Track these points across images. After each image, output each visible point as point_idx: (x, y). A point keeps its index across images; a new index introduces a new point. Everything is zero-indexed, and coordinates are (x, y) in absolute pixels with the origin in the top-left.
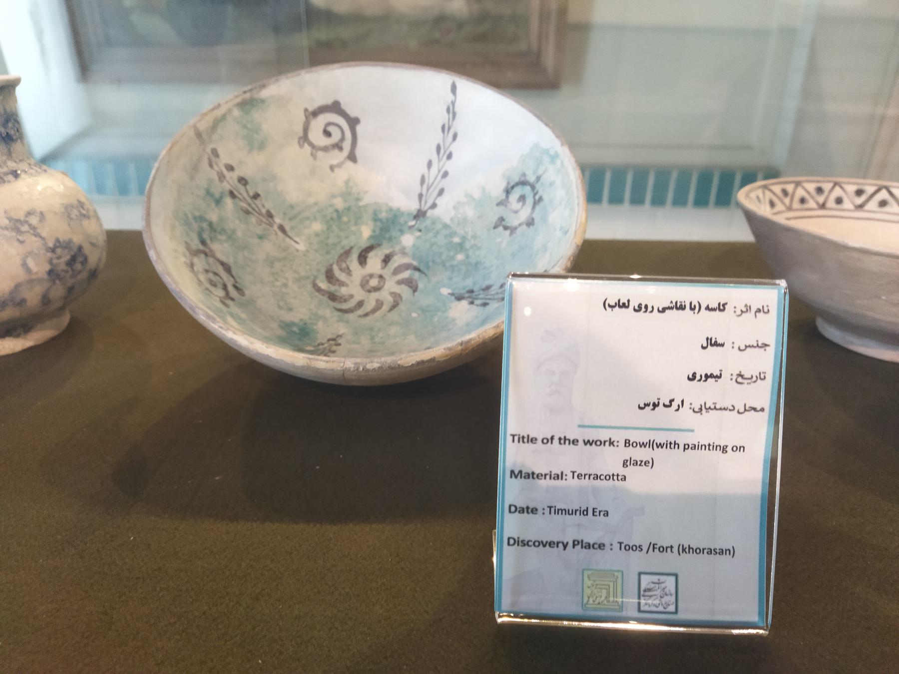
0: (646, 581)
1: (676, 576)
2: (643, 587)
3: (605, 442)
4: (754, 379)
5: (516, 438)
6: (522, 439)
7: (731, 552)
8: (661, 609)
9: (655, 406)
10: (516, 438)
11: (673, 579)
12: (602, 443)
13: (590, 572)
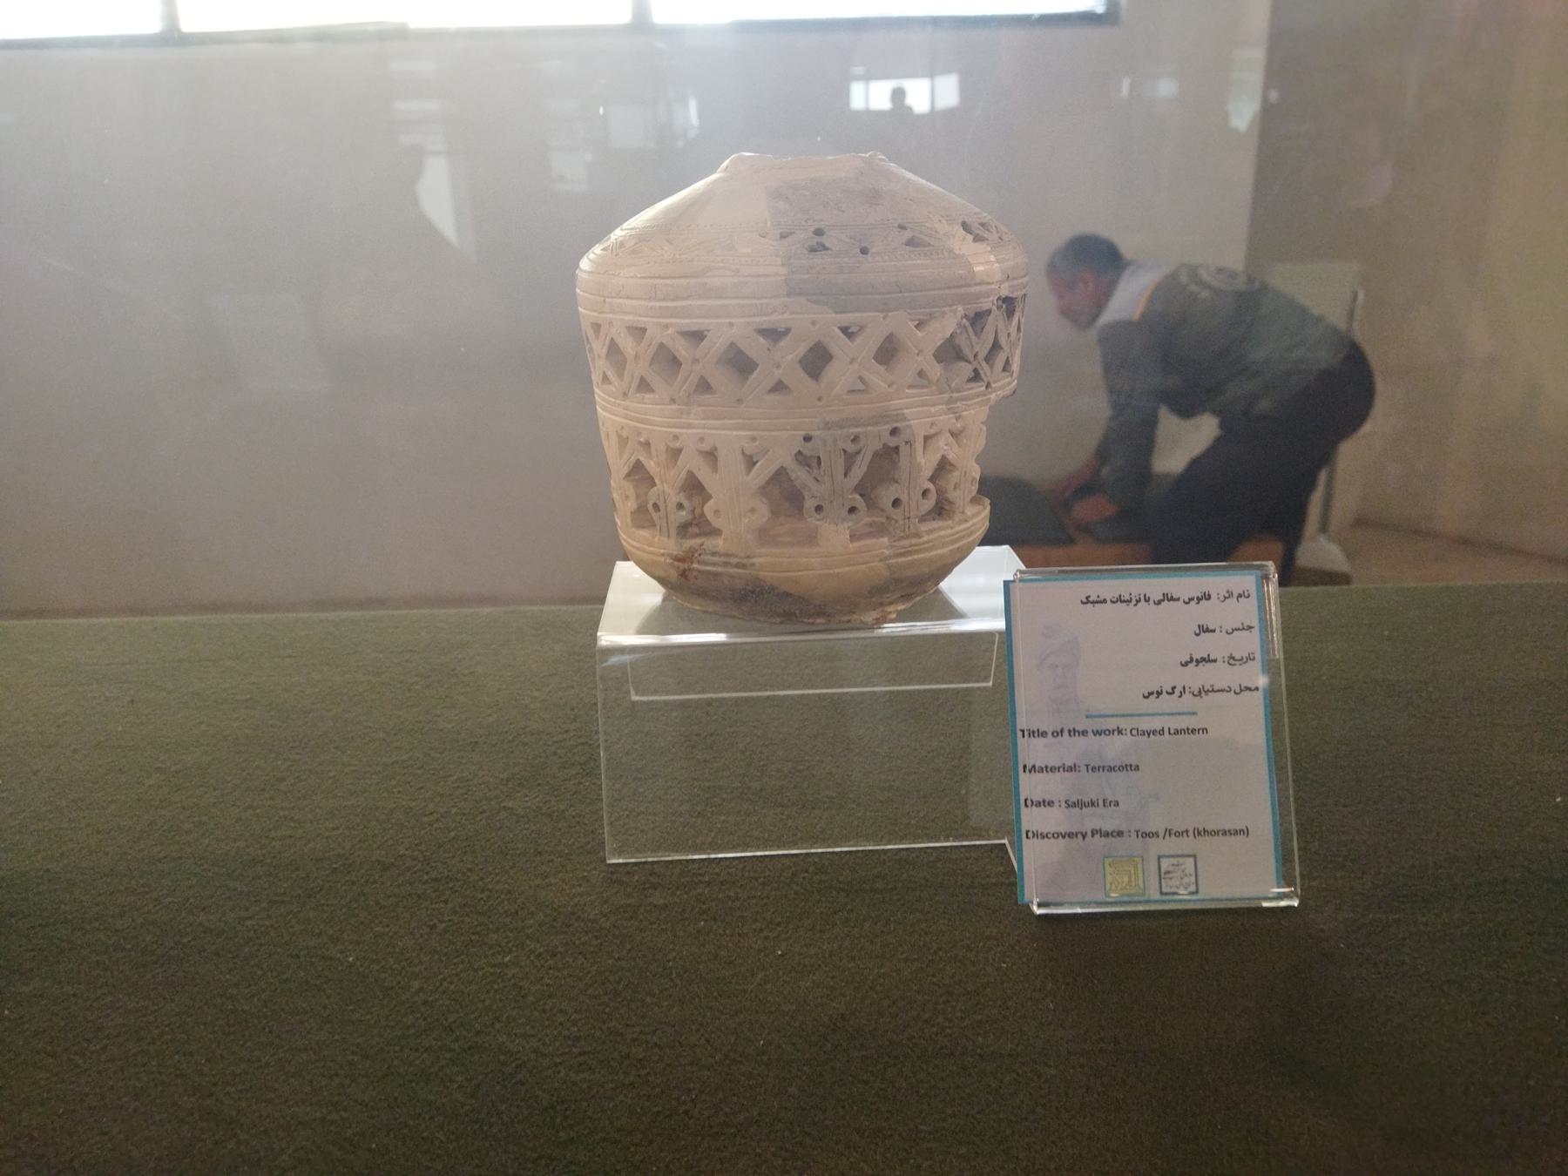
0: (1165, 864)
1: (1195, 857)
6: (1032, 734)
7: (1245, 832)
9: (1159, 694)
11: (1191, 860)
12: (1111, 732)
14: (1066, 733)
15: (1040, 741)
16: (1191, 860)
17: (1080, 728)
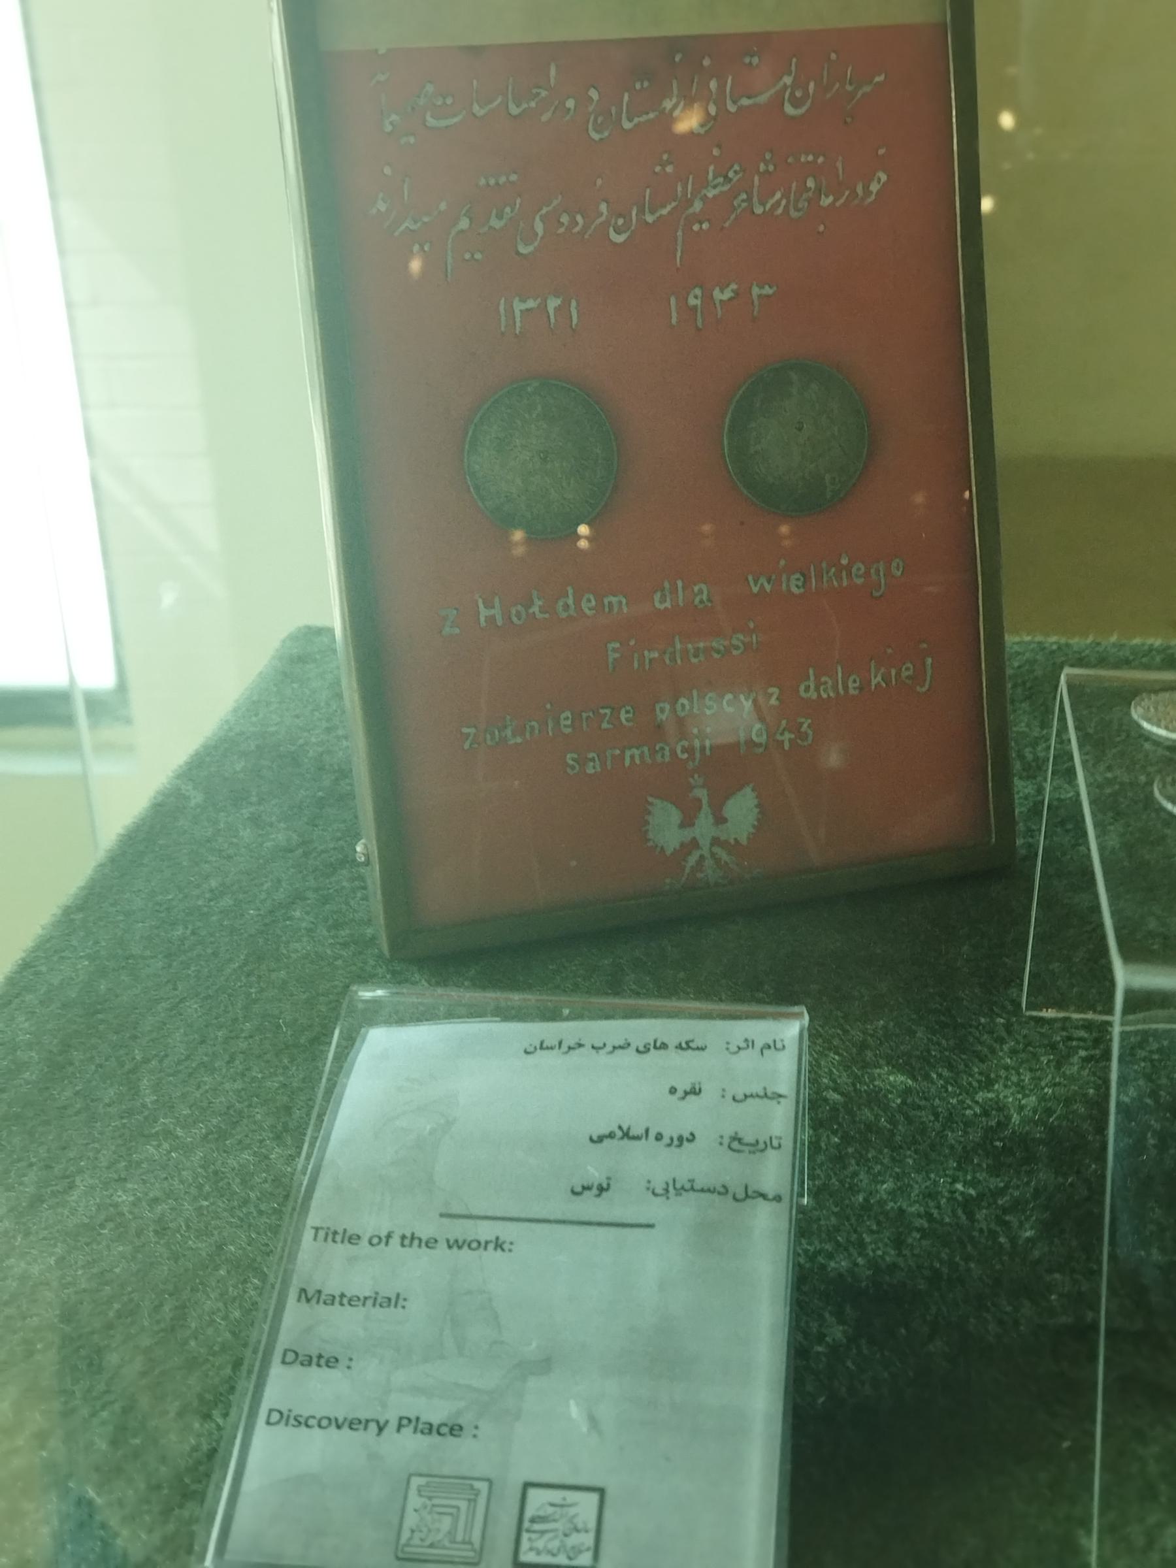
0: (538, 1500)
1: (601, 1491)
2: (529, 1512)
3: (487, 1243)
4: (762, 1146)
5: (321, 1234)
10: (321, 1234)
11: (594, 1498)
13: (422, 1481)
14: (395, 1241)
15: (342, 1250)
16: (594, 1498)
17: (424, 1233)
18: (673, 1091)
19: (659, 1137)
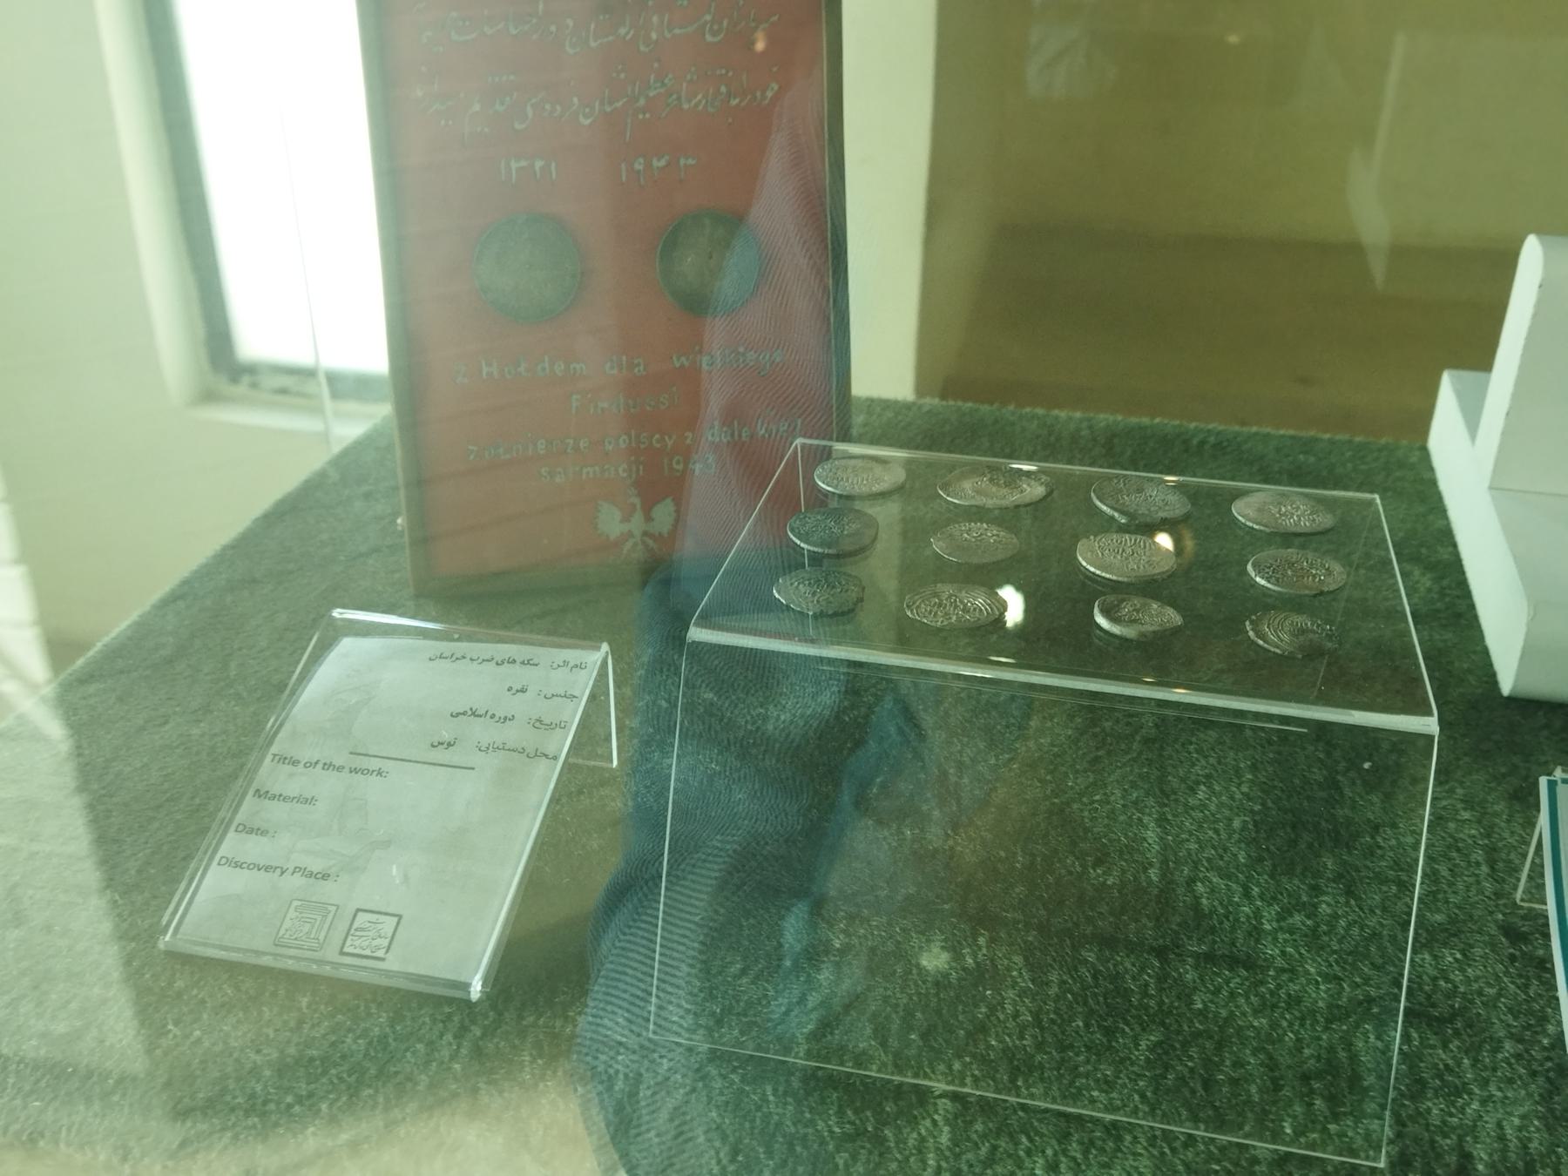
0: (362, 917)
1: (400, 917)
2: (356, 925)
8: (367, 952)
14: (320, 766)
15: (288, 768)
17: (337, 763)
18: (510, 689)
19: (493, 716)
